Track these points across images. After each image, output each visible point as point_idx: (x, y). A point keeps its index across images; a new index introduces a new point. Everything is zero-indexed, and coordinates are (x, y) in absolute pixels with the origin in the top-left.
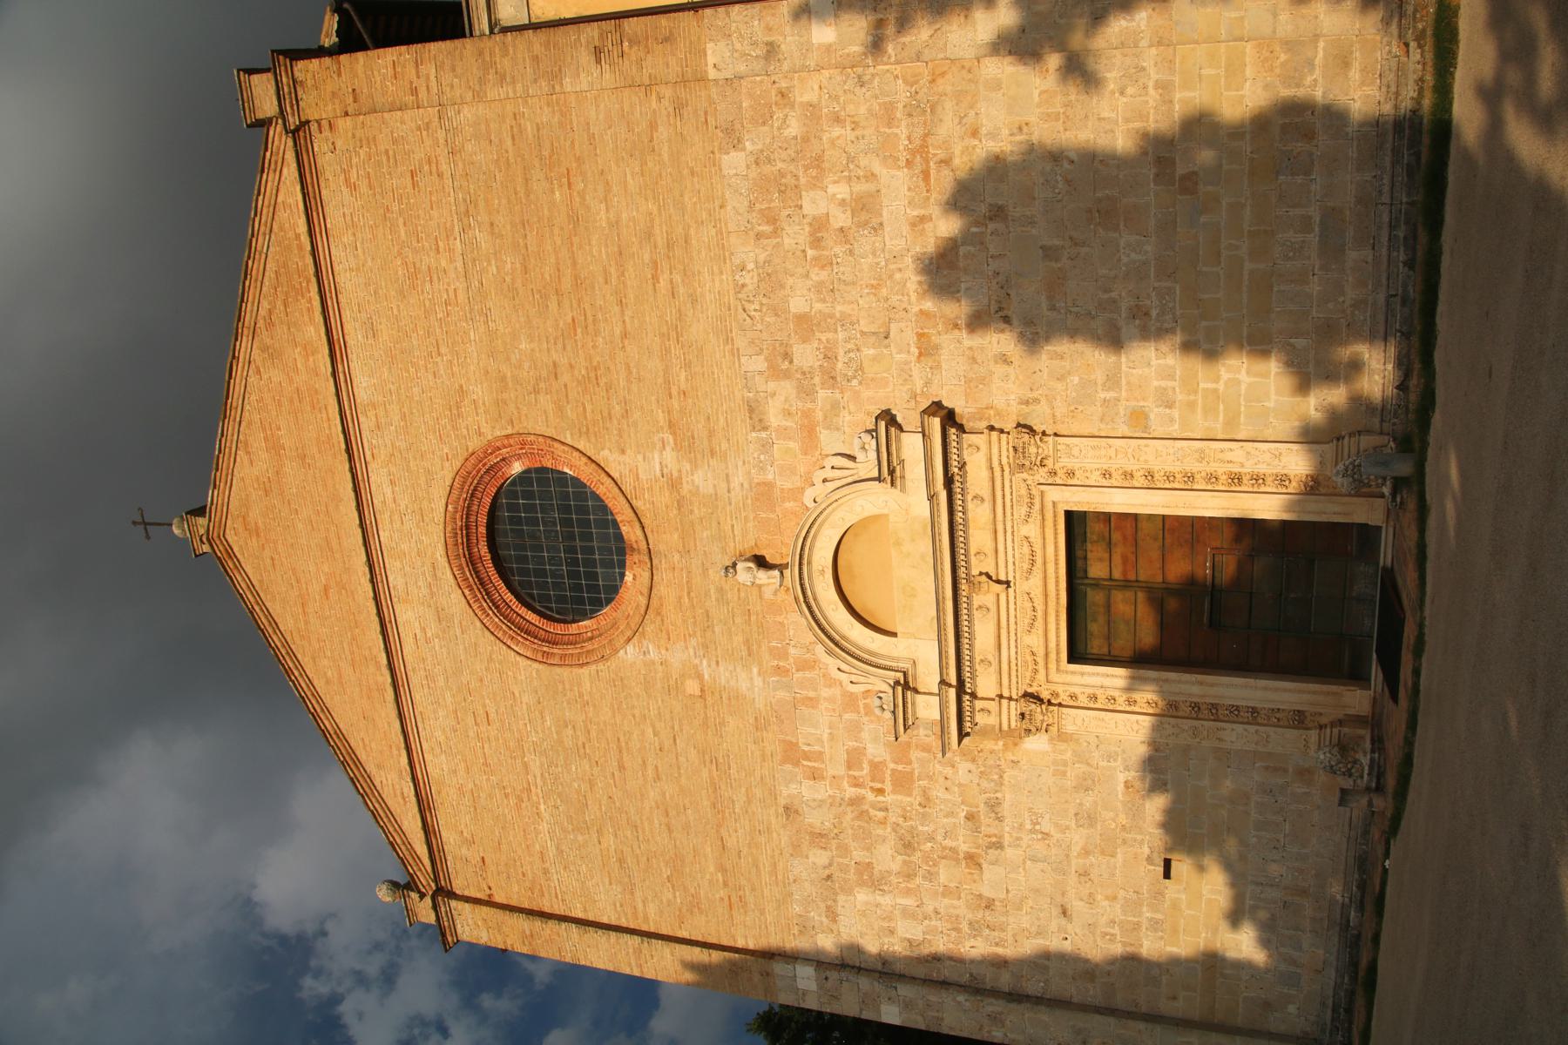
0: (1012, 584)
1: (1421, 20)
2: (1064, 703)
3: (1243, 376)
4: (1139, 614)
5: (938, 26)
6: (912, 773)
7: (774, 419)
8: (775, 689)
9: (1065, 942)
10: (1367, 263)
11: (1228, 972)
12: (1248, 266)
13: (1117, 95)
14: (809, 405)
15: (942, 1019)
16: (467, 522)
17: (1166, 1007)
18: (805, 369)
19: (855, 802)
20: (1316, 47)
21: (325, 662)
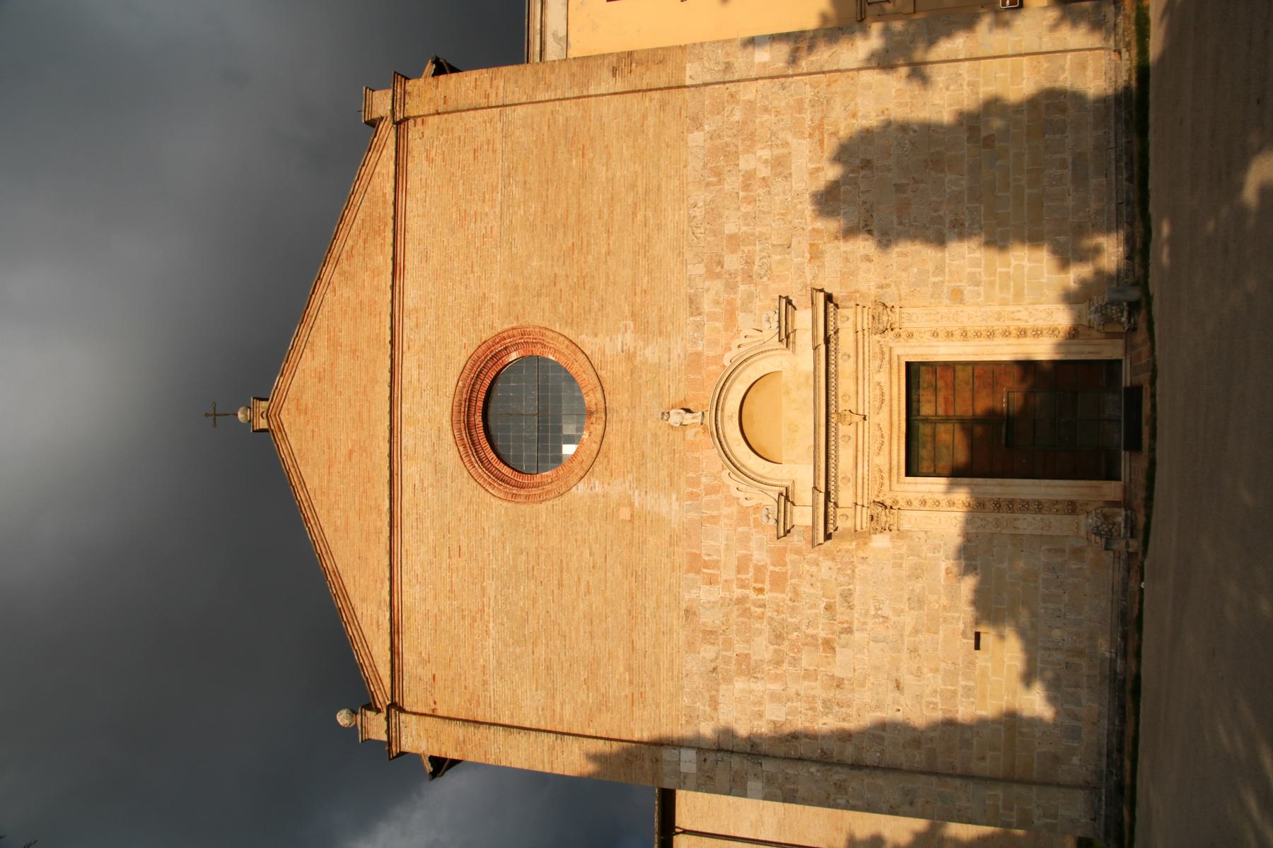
0: (867, 418)
1: (1128, 36)
3: (1026, 263)
4: (956, 440)
5: (834, 50)
6: (786, 573)
7: (707, 306)
8: (687, 512)
9: (897, 713)
10: (1103, 185)
11: (1024, 730)
12: (1027, 191)
13: (944, 90)
14: (732, 296)
15: (797, 791)
16: (470, 396)
17: (977, 767)
19: (741, 601)
20: (1066, 59)
21: (338, 513)
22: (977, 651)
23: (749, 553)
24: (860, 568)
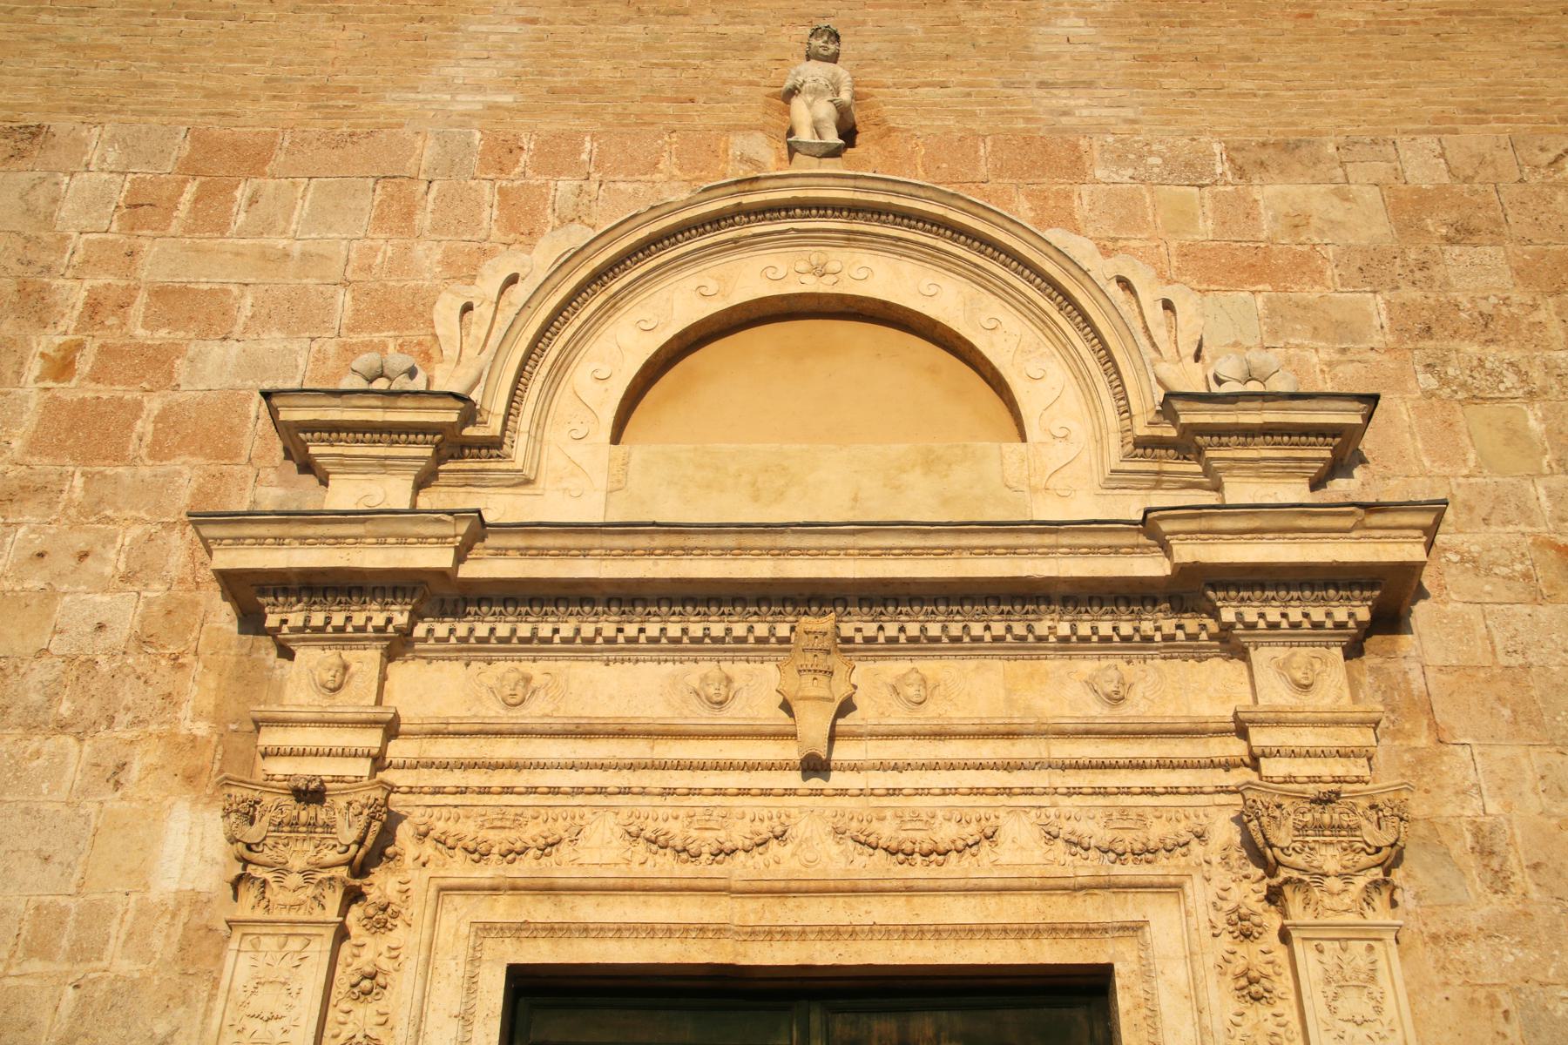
0: (815, 783)
2: (346, 949)
6: (119, 457)
18: (1437, 272)
23: (238, 329)
24: (74, 754)
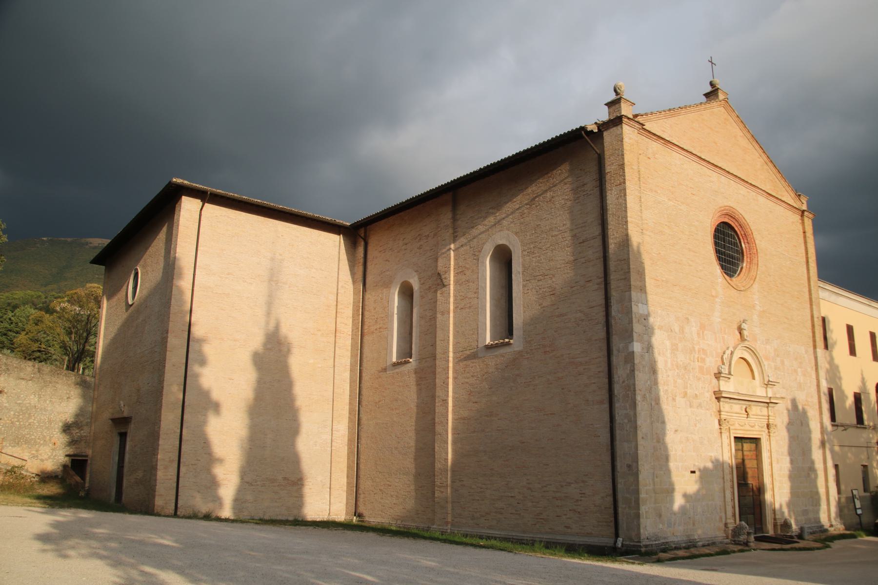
15: (640, 372)
22: (690, 472)
